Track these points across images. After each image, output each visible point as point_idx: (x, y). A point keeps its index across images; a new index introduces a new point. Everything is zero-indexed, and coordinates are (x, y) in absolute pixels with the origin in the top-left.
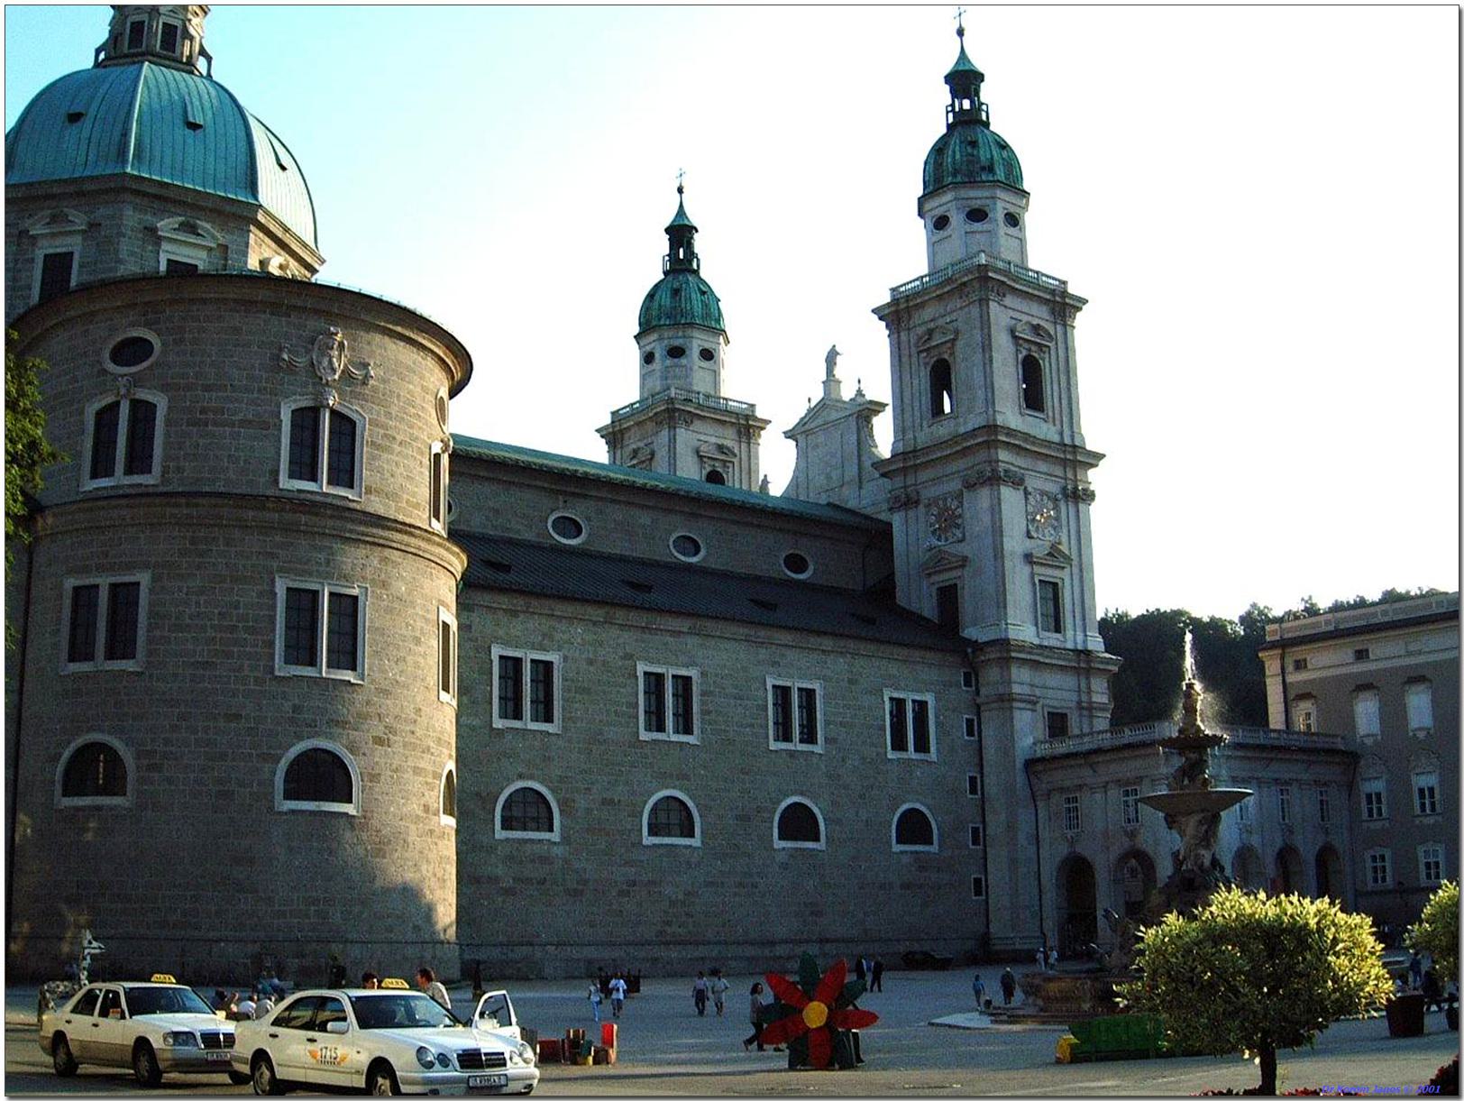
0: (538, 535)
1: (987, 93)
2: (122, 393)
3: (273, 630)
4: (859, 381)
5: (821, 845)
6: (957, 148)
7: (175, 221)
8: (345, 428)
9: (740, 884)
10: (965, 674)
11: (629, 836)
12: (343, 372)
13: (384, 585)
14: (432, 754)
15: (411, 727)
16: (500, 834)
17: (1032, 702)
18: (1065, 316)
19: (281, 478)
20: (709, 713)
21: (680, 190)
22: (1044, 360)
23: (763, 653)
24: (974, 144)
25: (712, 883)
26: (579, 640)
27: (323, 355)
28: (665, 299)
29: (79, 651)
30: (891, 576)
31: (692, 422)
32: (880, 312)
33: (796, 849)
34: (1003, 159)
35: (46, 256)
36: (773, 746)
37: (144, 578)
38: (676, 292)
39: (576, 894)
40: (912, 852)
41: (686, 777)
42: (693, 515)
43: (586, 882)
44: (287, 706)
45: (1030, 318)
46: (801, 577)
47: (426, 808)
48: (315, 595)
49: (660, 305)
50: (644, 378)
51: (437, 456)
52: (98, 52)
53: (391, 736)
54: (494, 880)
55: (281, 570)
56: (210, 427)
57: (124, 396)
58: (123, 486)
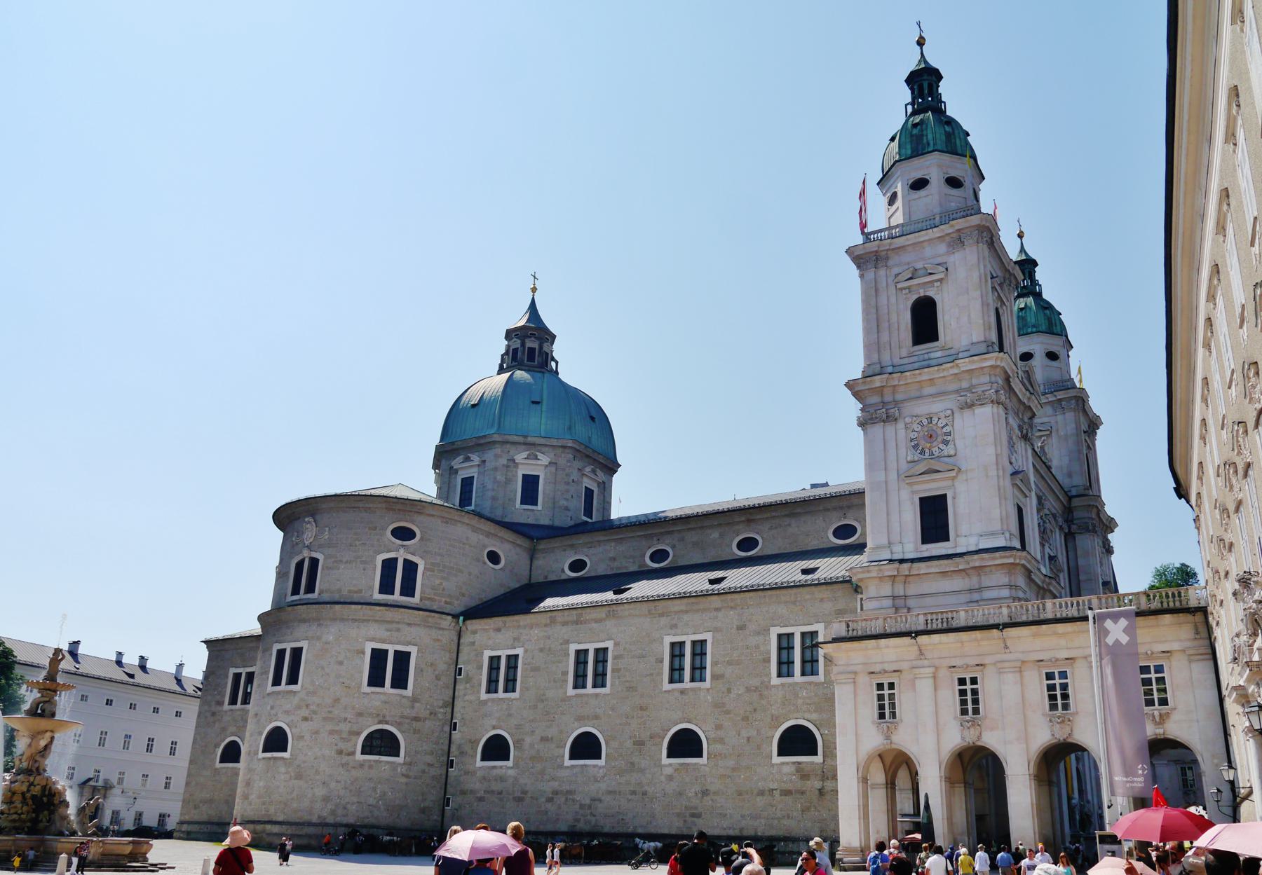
0: (640, 566)
7: (461, 458)
9: (634, 793)
11: (556, 760)
13: (319, 638)
14: (350, 722)
15: (330, 709)
16: (479, 763)
20: (618, 670)
21: (1021, 236)
23: (664, 621)
25: (610, 792)
39: (519, 800)
40: (794, 763)
41: (597, 717)
42: (749, 521)
43: (525, 792)
44: (269, 708)
47: (340, 752)
53: (313, 715)
54: (472, 792)
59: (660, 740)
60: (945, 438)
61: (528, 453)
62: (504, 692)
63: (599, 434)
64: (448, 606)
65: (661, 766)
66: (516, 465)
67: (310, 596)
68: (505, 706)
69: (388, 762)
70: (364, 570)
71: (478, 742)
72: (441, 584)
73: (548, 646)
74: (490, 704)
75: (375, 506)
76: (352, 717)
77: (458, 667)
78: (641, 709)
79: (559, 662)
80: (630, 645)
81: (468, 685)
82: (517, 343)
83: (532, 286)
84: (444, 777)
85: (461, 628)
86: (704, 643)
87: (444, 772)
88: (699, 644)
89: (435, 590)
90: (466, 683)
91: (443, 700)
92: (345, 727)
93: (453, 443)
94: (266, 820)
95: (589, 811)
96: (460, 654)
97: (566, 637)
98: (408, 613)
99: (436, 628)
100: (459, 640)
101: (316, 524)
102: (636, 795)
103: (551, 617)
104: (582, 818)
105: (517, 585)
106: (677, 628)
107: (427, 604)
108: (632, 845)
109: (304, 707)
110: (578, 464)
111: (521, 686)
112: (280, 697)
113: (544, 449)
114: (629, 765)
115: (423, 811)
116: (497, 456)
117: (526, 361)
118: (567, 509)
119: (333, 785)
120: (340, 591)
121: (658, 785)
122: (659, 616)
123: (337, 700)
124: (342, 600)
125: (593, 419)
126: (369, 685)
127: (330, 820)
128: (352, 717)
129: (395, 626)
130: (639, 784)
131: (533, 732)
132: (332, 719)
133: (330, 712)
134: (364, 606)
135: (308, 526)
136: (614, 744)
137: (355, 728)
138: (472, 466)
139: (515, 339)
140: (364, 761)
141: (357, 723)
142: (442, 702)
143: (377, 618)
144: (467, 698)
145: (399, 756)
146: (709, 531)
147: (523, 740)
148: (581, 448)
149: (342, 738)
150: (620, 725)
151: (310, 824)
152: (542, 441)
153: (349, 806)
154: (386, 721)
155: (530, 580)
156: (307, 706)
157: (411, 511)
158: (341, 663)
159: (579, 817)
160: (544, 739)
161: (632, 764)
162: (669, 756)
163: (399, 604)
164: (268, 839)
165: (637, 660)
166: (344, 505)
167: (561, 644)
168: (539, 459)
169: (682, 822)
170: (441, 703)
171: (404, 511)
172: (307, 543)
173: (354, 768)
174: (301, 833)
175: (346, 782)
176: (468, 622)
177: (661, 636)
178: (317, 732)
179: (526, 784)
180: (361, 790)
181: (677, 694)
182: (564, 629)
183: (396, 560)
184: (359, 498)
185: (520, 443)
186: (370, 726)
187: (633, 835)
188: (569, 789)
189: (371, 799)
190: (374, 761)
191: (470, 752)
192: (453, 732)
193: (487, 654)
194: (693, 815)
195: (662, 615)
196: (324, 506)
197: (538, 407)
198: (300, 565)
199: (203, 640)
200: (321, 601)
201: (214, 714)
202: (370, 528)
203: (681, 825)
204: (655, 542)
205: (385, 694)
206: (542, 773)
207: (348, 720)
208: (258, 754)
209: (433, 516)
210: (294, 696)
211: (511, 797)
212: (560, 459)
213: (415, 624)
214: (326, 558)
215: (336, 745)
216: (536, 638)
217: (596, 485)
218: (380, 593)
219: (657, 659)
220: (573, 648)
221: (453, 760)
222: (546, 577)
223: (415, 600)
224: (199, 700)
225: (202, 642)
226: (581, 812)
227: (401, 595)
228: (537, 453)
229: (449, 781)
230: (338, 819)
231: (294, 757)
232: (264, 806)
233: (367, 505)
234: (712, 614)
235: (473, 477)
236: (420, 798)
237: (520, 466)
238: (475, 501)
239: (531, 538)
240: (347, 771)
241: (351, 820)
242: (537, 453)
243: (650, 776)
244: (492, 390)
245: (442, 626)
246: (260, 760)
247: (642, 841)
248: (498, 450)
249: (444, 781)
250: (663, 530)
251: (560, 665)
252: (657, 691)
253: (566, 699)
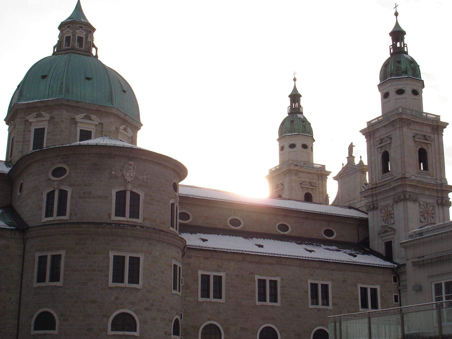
1: (407, 39)
2: (56, 187)
3: (108, 271)
4: (361, 157)
6: (392, 65)
7: (82, 115)
8: (135, 197)
10: (394, 277)
12: (135, 177)
17: (320, 305)
18: (438, 131)
19: (112, 216)
21: (295, 80)
22: (428, 149)
24: (399, 62)
27: (127, 172)
28: (288, 125)
29: (41, 278)
30: (368, 238)
31: (298, 174)
32: (364, 132)
34: (412, 67)
35: (35, 129)
36: (311, 306)
37: (63, 253)
38: (292, 122)
44: (113, 298)
45: (422, 133)
46: (331, 238)
48: (124, 257)
49: (286, 127)
50: (281, 155)
51: (173, 205)
52: (54, 47)
55: (112, 249)
56: (87, 199)
57: (56, 188)
58: (56, 220)
60: (432, 215)
74: (205, 304)
133: (160, 306)
138: (91, 124)
144: (187, 298)
156: (147, 300)
160: (243, 329)
178: (154, 319)
198: (121, 196)
208: (107, 331)
214: (145, 195)
215: (164, 328)
216: (232, 268)
246: (110, 336)
248: (112, 120)
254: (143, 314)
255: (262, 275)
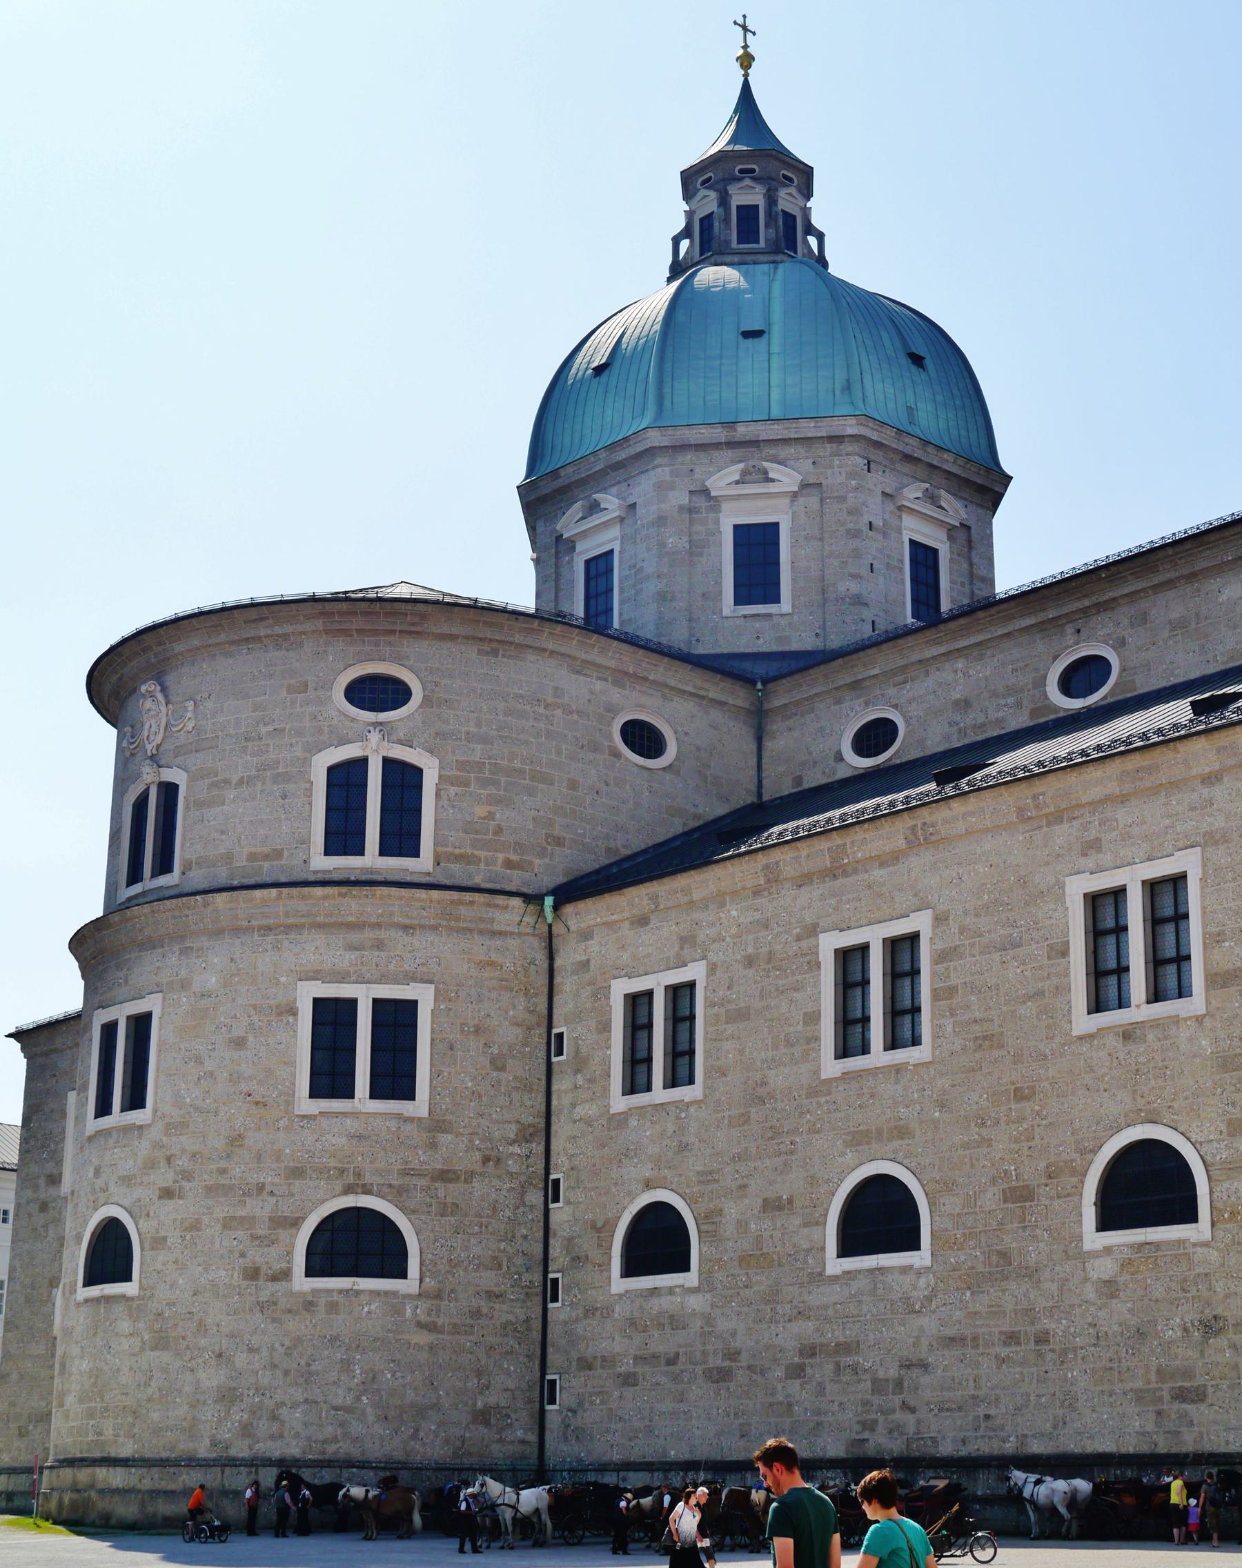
0: (1034, 713)
5: (1199, 1231)
7: (577, 509)
9: (1012, 1338)
13: (185, 985)
15: (223, 1164)
16: (619, 1284)
20: (951, 991)
23: (1063, 833)
25: (951, 1341)
26: (734, 930)
33: (1139, 1247)
39: (721, 1376)
41: (902, 1132)
43: (733, 1355)
44: (91, 1175)
47: (253, 1274)
53: (184, 1183)
54: (608, 1361)
59: (1074, 1180)
61: (742, 465)
62: (665, 1088)
63: (939, 398)
64: (516, 874)
65: (1085, 1257)
66: (715, 503)
67: (164, 880)
68: (671, 1127)
69: (377, 1293)
70: (284, 797)
71: (611, 1225)
72: (491, 816)
73: (765, 950)
74: (633, 1122)
75: (300, 628)
76: (277, 1180)
77: (555, 1031)
78: (1019, 1095)
79: (796, 990)
80: (977, 915)
81: (580, 1079)
82: (709, 202)
83: (741, 52)
84: (537, 1325)
85: (550, 926)
86: (1180, 885)
87: (538, 1310)
88: (1169, 888)
89: (477, 833)
90: (577, 1071)
91: (518, 1122)
92: (260, 1208)
93: (555, 473)
94: (97, 1454)
95: (897, 1400)
96: (555, 999)
97: (809, 918)
98: (401, 898)
99: (481, 932)
100: (551, 958)
101: (166, 697)
102: (1019, 1344)
103: (767, 867)
104: (881, 1419)
105: (721, 810)
106: (1099, 849)
107: (458, 873)
108: (1002, 1490)
109: (163, 1164)
110: (880, 480)
111: (705, 1067)
112: (111, 1142)
113: (785, 452)
114: (994, 1259)
115: (483, 1417)
116: (660, 487)
117: (734, 245)
118: (859, 601)
119: (241, 1359)
120: (228, 857)
121: (1077, 1311)
122: (1049, 824)
123: (236, 1140)
124: (235, 883)
125: (917, 360)
126: (314, 1094)
127: (241, 1450)
128: (277, 1180)
129: (369, 934)
130: (1028, 1311)
131: (743, 1187)
132: (227, 1190)
133: (223, 1171)
134: (285, 891)
135: (148, 704)
136: (952, 1204)
137: (286, 1210)
139: (703, 192)
140: (315, 1292)
141: (293, 1195)
142: (514, 1127)
143: (320, 919)
144: (580, 1111)
145: (403, 1275)
146: (1213, 584)
147: (720, 1212)
148: (887, 437)
149: (255, 1237)
150: (966, 1146)
151: (192, 1462)
152: (776, 431)
153: (284, 1412)
154: (364, 1186)
155: (760, 795)
156: (169, 1160)
157: (393, 632)
158: (240, 1043)
159: (873, 1416)
160: (772, 1206)
161: (1003, 1255)
162: (1104, 1224)
163: (380, 878)
164: (103, 1505)
165: (996, 956)
166: (223, 637)
167: (799, 939)
168: (773, 480)
169: (1152, 1417)
170: (511, 1131)
171: (375, 632)
172: (150, 748)
173: (290, 1311)
174: (172, 1486)
175: (272, 1348)
176: (569, 909)
177: (1058, 881)
178: (195, 1226)
179: (734, 1334)
180: (313, 1368)
181: (1112, 1041)
182: (804, 895)
183: (363, 762)
184: (253, 614)
185: (717, 446)
186: (323, 1201)
187: (1003, 1463)
188: (842, 1339)
189: (340, 1392)
190: (340, 1292)
191: (595, 1255)
192: (552, 1206)
193: (621, 988)
194: (1181, 1395)
195: (1057, 818)
196: (179, 648)
197: (759, 344)
199: (13, 1030)
200: (189, 889)
201: (44, 1207)
202: (290, 689)
203: (1150, 1427)
204: (1070, 638)
205: (355, 1115)
206: (772, 1298)
207: (268, 1188)
209: (452, 638)
210: (140, 1136)
211: (699, 1370)
212: (829, 472)
213: (422, 927)
214: (193, 778)
215: (243, 1255)
216: (734, 930)
217: (943, 535)
218: (327, 853)
219: (1051, 947)
220: (830, 943)
221: (557, 1279)
222: (798, 780)
223: (422, 864)
224: (15, 1173)
225: (10, 1036)
226: (876, 1400)
227: (383, 852)
228: (766, 465)
229: (550, 1336)
230: (86, 1455)
231: (148, 1293)
232: (92, 1422)
233: (278, 630)
234: (1195, 795)
235: (612, 551)
236: (472, 1383)
237: (725, 506)
238: (621, 614)
239: (748, 681)
240: (274, 1320)
241: (293, 1449)
242: (766, 465)
243: (1054, 1287)
244: (642, 323)
245: (496, 927)
246: (78, 1305)
247: (1033, 1478)
248: (661, 471)
249: (536, 1335)
250: (1086, 602)
251: (797, 996)
252: (1057, 1039)
253: (819, 1088)
254: (152, 1214)
255: (849, 928)
